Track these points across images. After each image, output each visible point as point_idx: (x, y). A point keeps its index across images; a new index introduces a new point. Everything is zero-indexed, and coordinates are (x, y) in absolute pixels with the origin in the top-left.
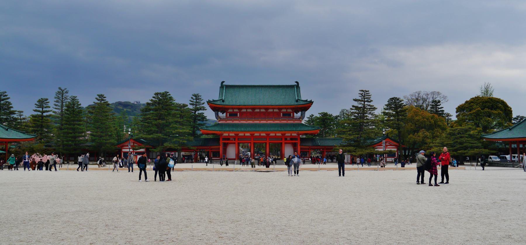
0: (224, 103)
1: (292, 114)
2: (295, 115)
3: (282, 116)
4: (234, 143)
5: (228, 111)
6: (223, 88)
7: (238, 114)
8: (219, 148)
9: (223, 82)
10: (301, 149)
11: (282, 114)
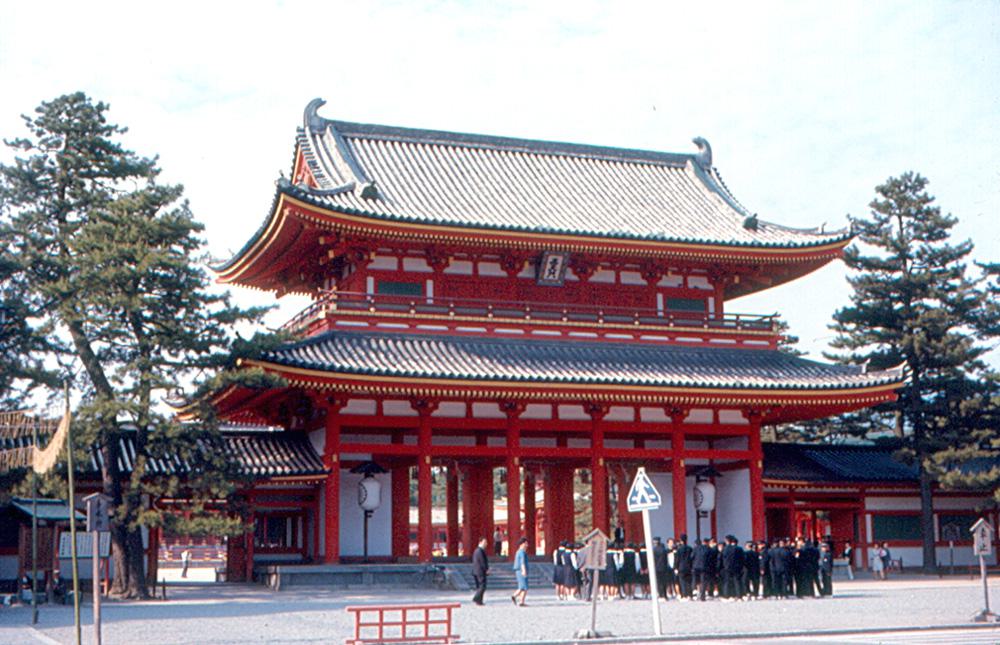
1: (711, 301)
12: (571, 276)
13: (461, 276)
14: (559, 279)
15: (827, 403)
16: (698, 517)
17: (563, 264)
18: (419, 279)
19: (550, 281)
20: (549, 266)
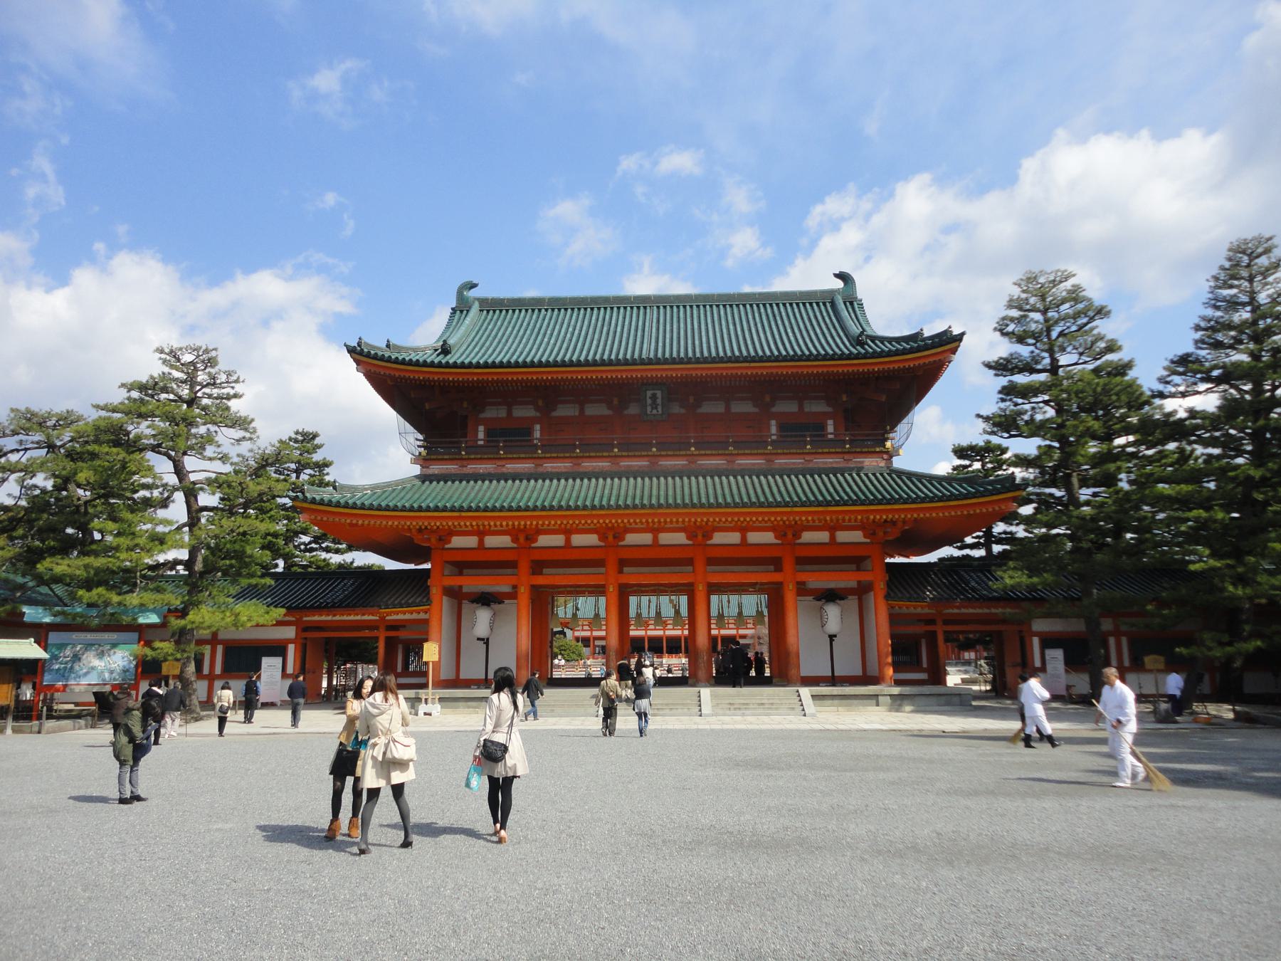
0: (451, 359)
5: (482, 416)
6: (468, 311)
8: (426, 622)
9: (473, 286)
10: (894, 619)
11: (773, 422)
12: (676, 409)
14: (663, 414)
17: (662, 398)
19: (654, 415)
20: (649, 401)
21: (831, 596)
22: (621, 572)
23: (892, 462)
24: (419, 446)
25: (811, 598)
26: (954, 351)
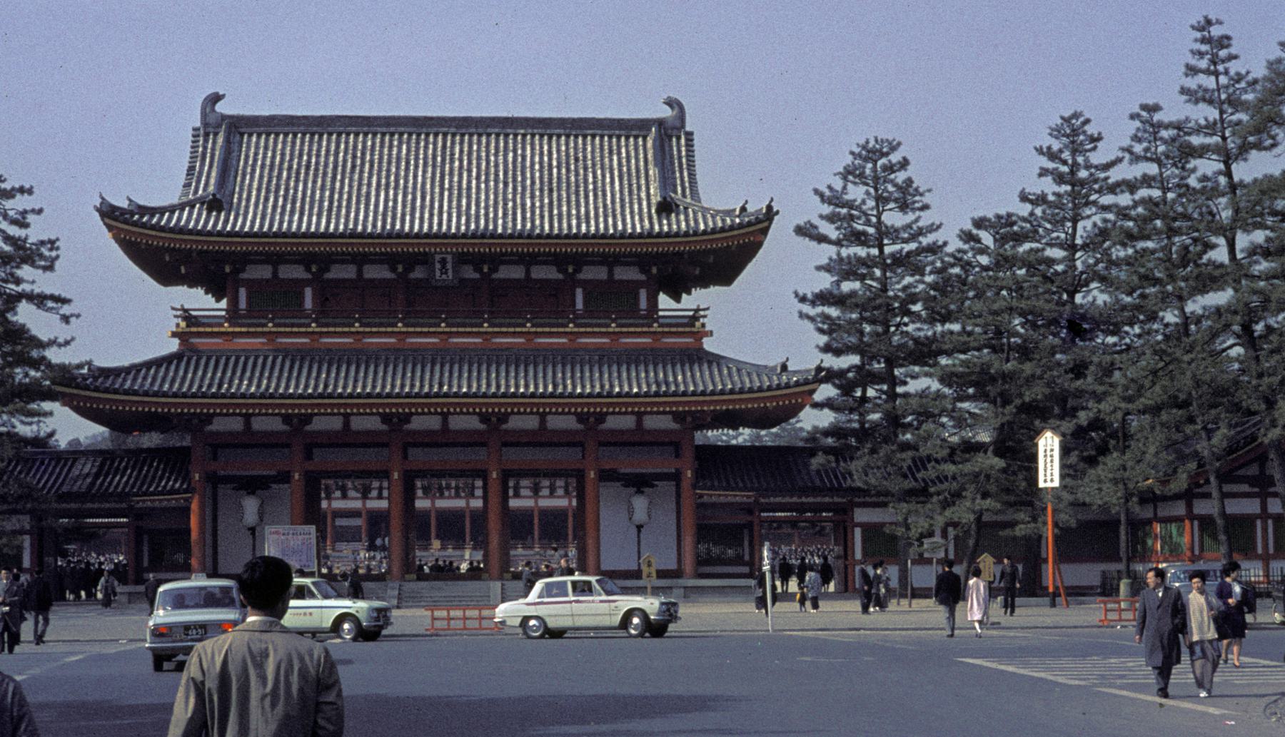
1: (643, 295)
2: (661, 306)
3: (580, 304)
4: (284, 478)
5: (244, 276)
7: (308, 292)
13: (344, 281)
15: (759, 407)
16: (639, 531)
18: (296, 287)
19: (444, 280)
20: (438, 266)
21: (640, 483)
22: (405, 457)
23: (702, 344)
24: (176, 316)
25: (618, 484)
26: (765, 231)
